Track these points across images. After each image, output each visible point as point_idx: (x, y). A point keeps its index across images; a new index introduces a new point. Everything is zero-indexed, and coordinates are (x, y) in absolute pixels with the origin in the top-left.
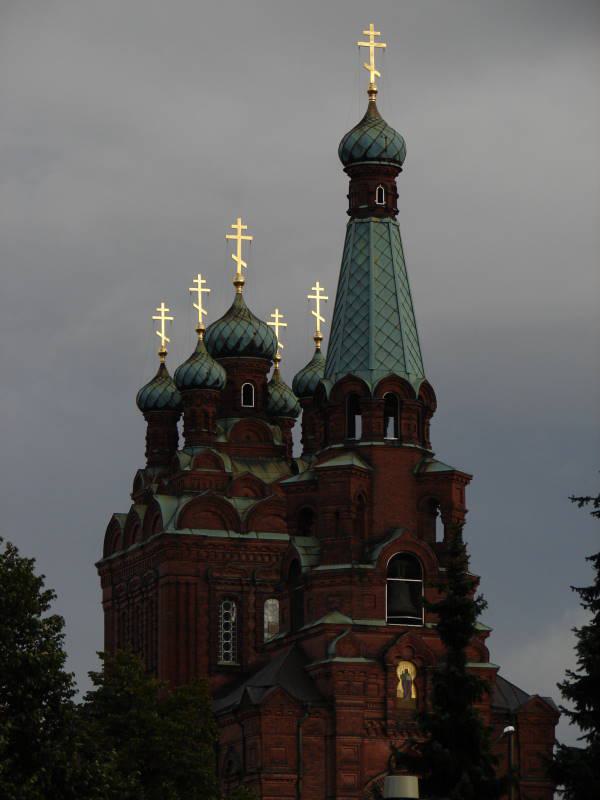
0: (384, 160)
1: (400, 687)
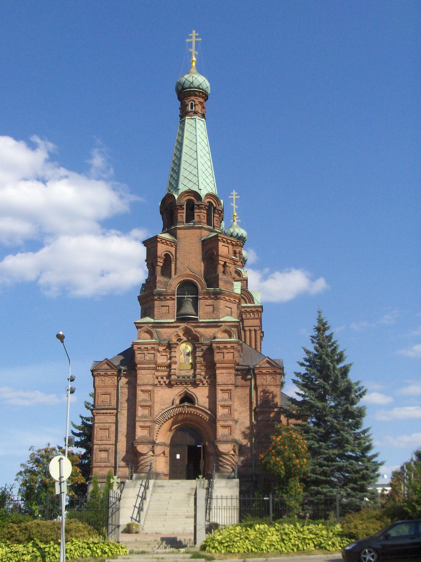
0: (192, 88)
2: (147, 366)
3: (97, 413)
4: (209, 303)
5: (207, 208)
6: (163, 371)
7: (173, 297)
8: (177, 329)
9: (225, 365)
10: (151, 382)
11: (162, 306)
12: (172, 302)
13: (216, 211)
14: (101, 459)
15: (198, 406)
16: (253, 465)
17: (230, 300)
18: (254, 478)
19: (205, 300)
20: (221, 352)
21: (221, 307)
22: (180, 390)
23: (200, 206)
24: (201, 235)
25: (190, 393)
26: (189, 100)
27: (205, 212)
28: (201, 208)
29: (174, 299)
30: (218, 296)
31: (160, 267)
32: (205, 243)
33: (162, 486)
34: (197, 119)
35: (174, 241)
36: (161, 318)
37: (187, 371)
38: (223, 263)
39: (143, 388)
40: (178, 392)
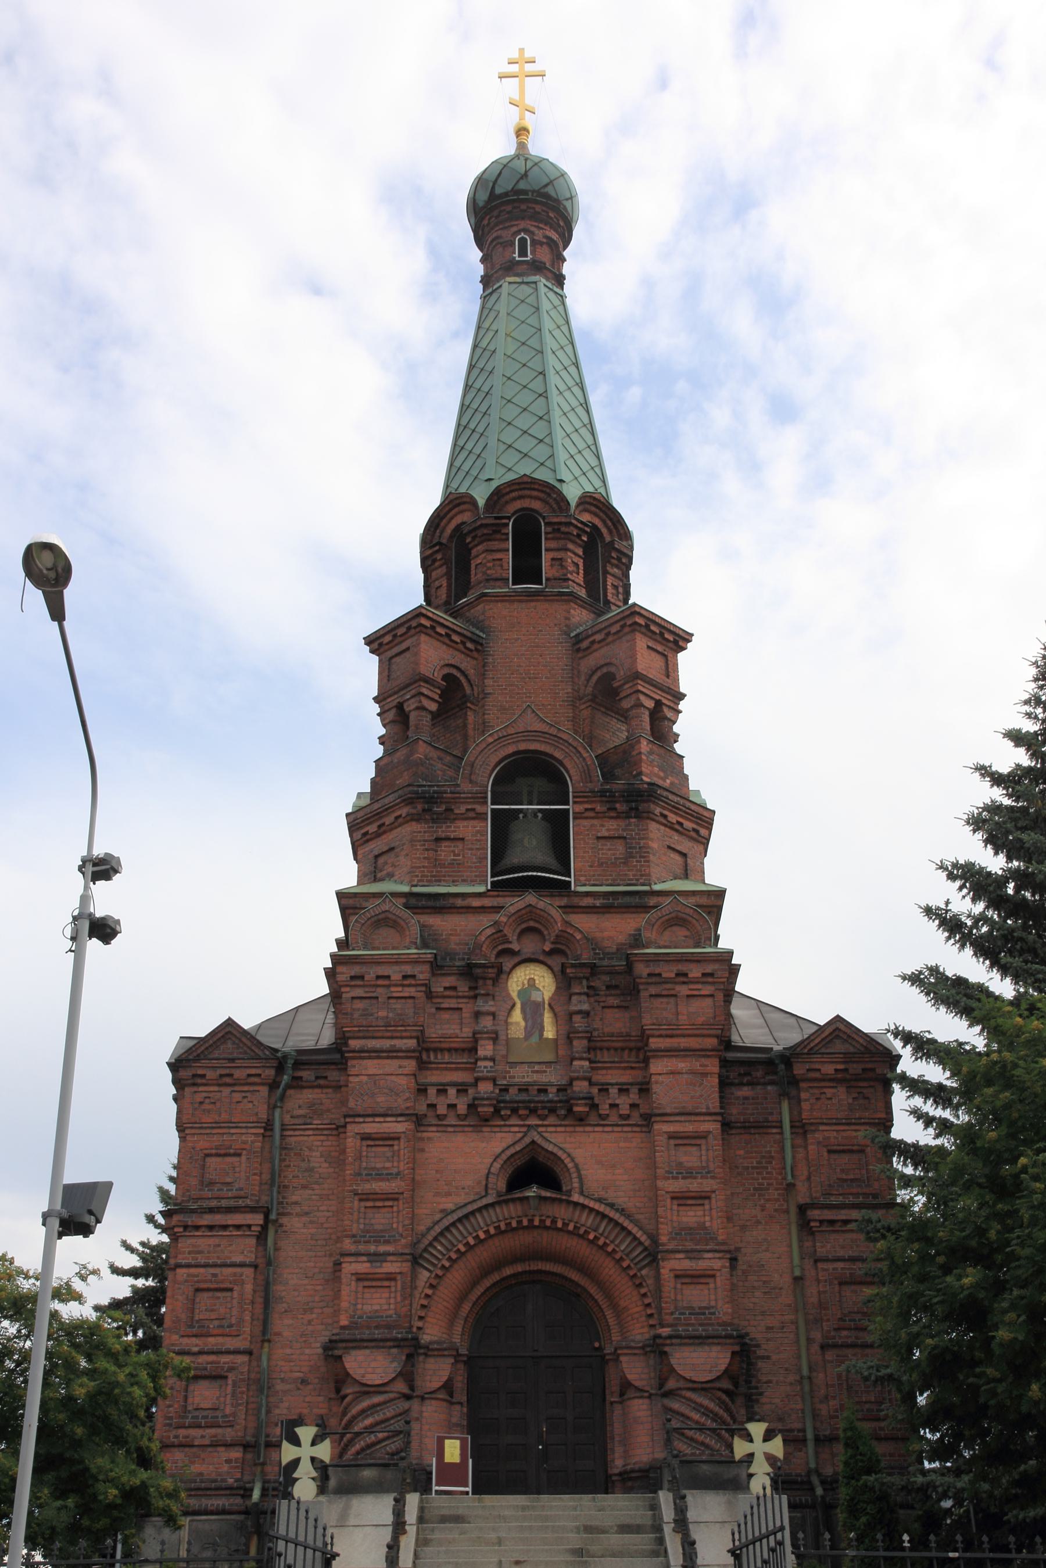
1: (517, 1016)
2: (387, 1044)
3: (186, 1227)
4: (608, 830)
5: (585, 539)
6: (446, 1069)
7: (479, 808)
8: (497, 917)
9: (684, 1042)
10: (401, 1103)
11: (438, 840)
12: (478, 825)
13: (614, 555)
14: (197, 1413)
15: (581, 1200)
16: (810, 1435)
17: (681, 824)
18: (819, 1491)
19: (595, 822)
20: (664, 993)
21: (654, 845)
22: (509, 1139)
23: (563, 529)
24: (568, 619)
25: (550, 1148)
26: (515, 229)
27: (580, 551)
28: (567, 536)
29: (481, 817)
30: (642, 807)
31: (429, 717)
32: (585, 644)
33: (458, 1519)
34: (541, 286)
35: (475, 637)
36: (438, 880)
37: (537, 1068)
38: (650, 704)
39: (371, 1127)
40: (504, 1145)
